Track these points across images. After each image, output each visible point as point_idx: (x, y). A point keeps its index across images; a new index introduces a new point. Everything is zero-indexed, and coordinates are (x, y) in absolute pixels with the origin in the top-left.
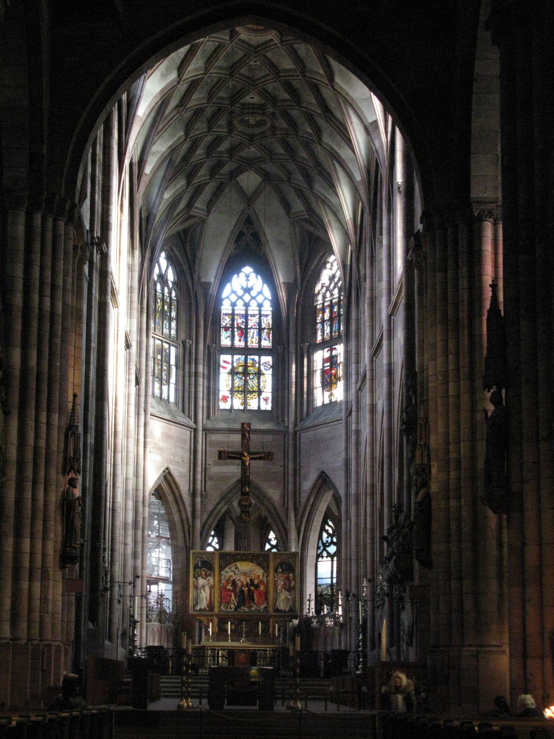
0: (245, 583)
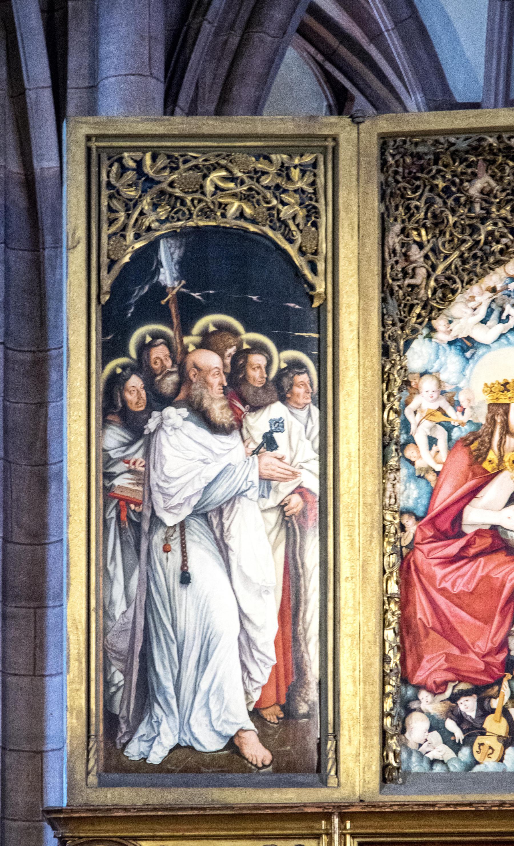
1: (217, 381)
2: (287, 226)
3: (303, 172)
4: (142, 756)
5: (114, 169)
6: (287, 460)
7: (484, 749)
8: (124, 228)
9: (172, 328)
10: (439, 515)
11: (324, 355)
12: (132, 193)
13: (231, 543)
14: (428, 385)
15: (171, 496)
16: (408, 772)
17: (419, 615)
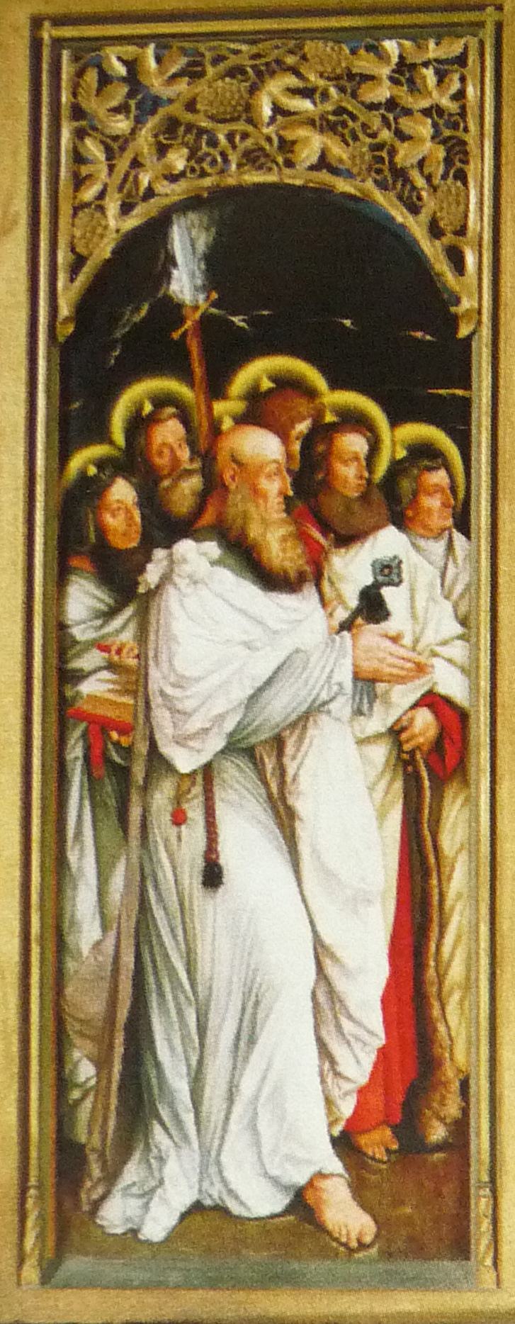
1: (274, 487)
2: (407, 180)
3: (441, 77)
4: (130, 1226)
6: (407, 641)
9: (191, 384)
12: (121, 125)
13: (301, 805)
15: (187, 715)
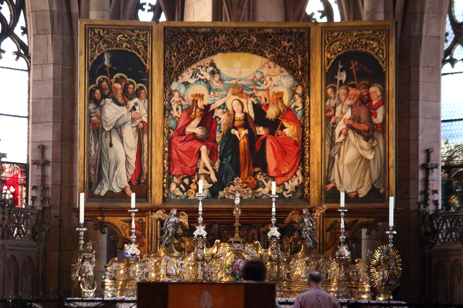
0: (239, 115)
1: (120, 92)
3: (143, 36)
5: (93, 33)
6: (139, 113)
7: (190, 193)
8: (95, 49)
10: (179, 129)
11: (149, 84)
12: (97, 40)
13: (124, 136)
14: (176, 94)
15: (107, 123)
16: (171, 198)
17: (174, 156)
